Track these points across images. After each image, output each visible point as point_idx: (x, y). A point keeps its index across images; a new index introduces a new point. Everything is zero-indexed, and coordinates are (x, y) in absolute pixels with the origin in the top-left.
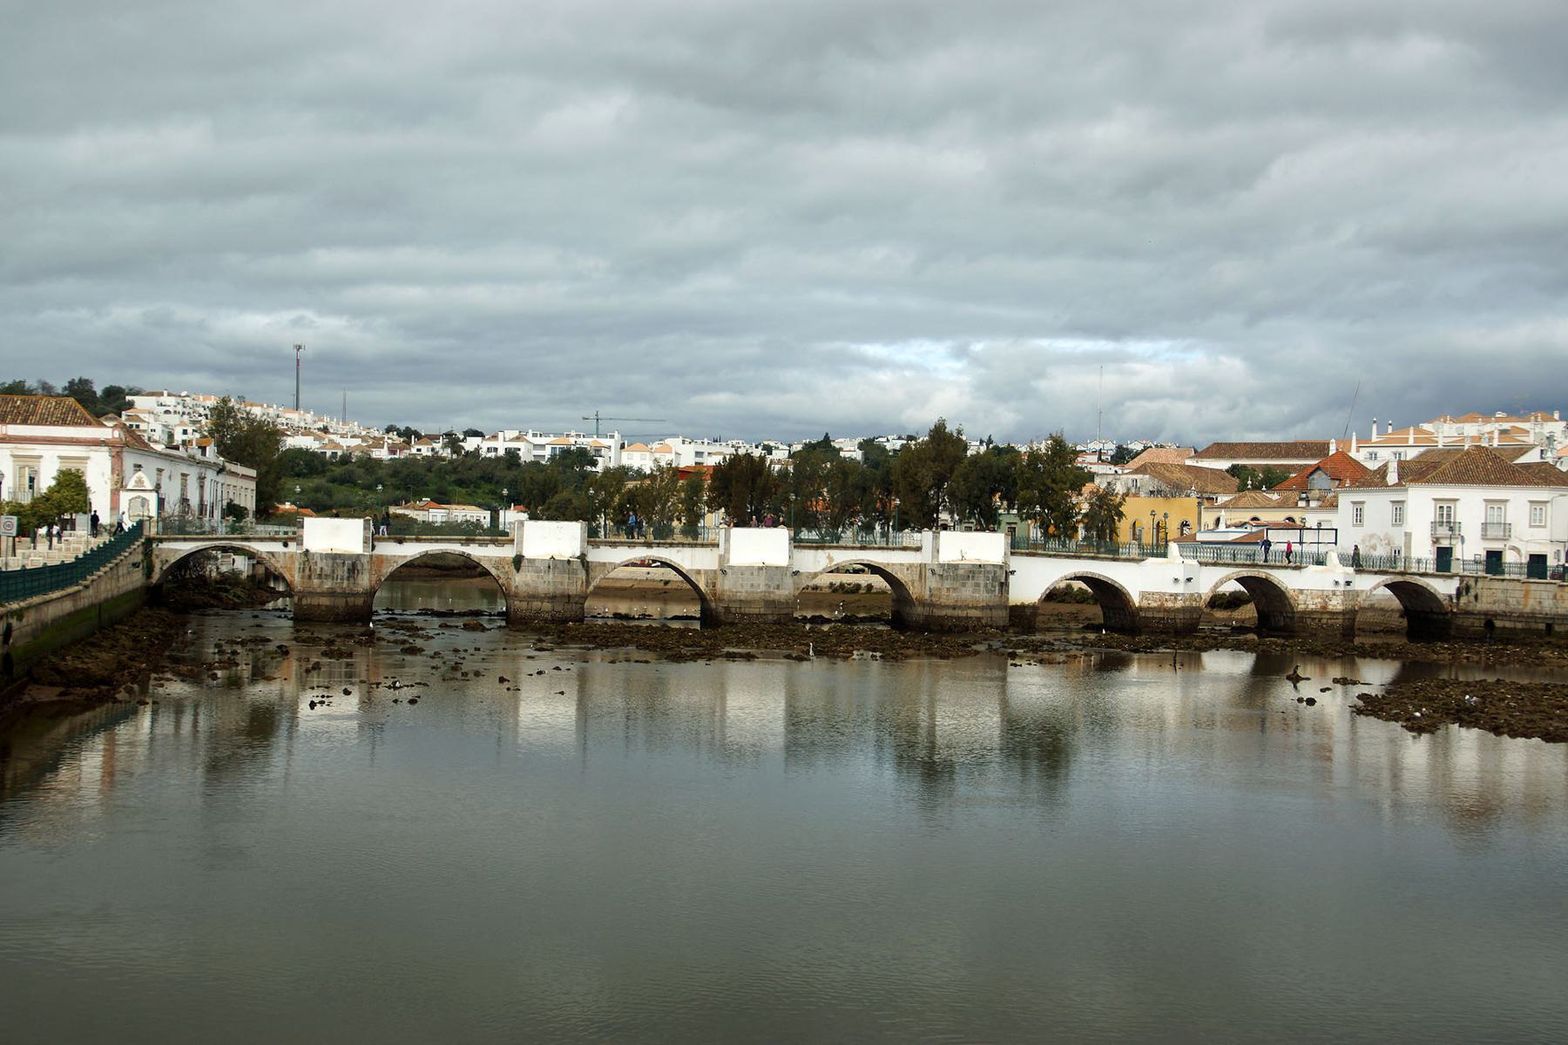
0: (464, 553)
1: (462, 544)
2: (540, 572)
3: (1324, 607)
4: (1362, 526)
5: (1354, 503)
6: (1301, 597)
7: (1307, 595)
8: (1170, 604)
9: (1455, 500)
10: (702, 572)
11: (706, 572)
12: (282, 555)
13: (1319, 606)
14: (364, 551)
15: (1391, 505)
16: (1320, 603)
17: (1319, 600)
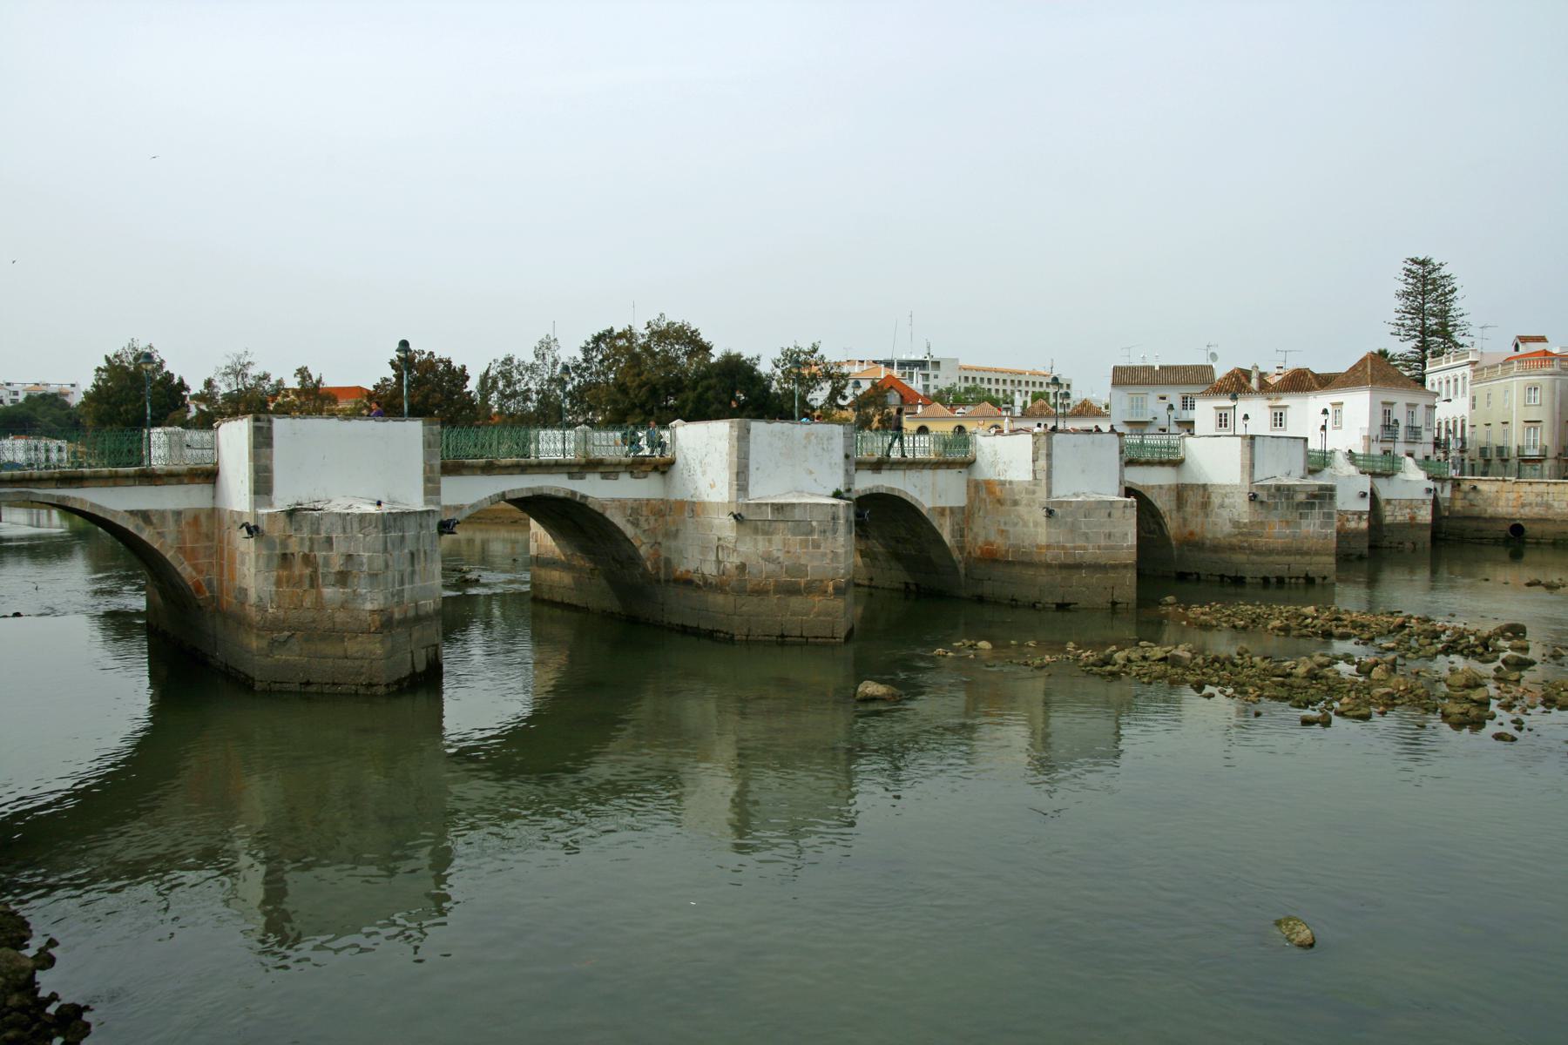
0: (574, 493)
1: (571, 476)
2: (811, 532)
3: (1413, 518)
4: (1340, 428)
5: (1216, 408)
6: (1388, 508)
7: (1395, 506)
9: (1286, 407)
10: (948, 512)
11: (952, 509)
12: (171, 520)
13: (1408, 516)
14: (427, 502)
15: (1214, 411)
16: (1409, 514)
17: (1408, 510)
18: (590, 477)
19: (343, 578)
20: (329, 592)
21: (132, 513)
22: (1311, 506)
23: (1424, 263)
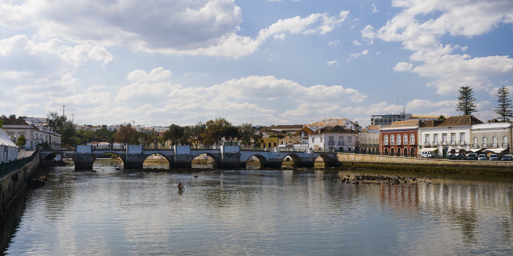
1: (114, 151)
6: (303, 159)
8: (275, 161)
18: (116, 151)
19: (81, 159)
20: (80, 160)
21: (68, 154)
22: (231, 156)
23: (466, 88)
